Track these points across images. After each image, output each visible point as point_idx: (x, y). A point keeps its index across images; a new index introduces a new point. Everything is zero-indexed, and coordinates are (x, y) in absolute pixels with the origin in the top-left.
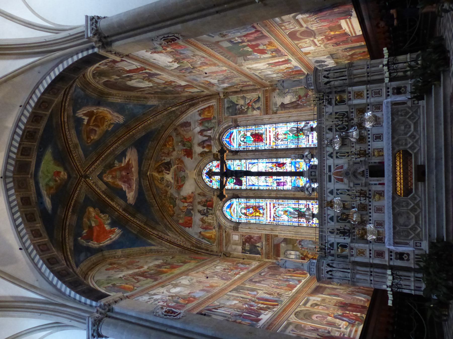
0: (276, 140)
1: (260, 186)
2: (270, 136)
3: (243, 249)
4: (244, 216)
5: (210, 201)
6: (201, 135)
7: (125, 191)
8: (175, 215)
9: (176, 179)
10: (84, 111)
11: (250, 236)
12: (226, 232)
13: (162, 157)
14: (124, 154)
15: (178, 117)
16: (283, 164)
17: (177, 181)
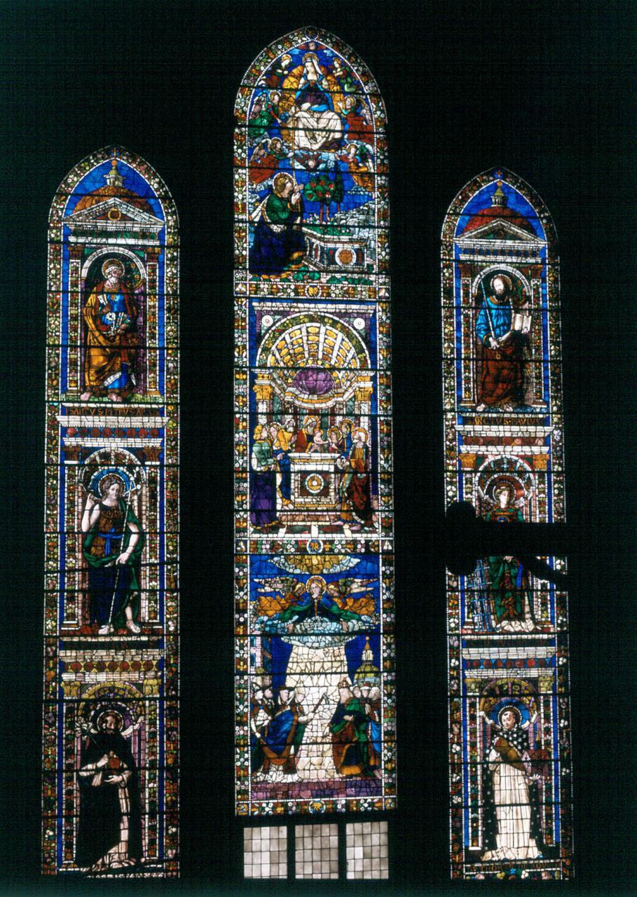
0: (487, 471)
1: (254, 377)
4: (84, 273)
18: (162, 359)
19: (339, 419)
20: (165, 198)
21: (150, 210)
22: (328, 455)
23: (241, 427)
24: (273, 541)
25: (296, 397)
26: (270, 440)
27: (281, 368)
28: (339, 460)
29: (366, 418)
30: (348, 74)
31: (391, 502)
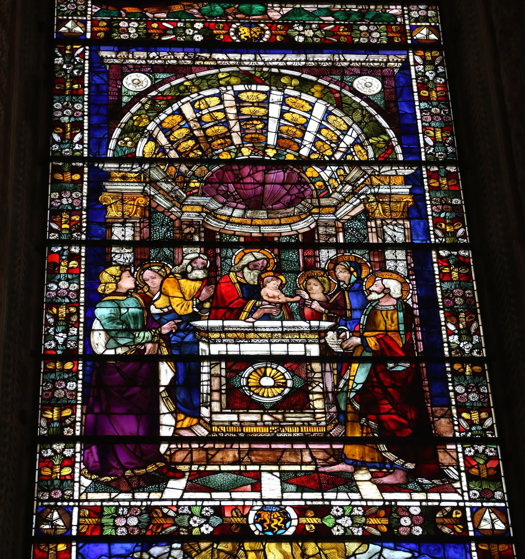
19: (325, 255)
22: (303, 324)
23: (63, 270)
24: (150, 510)
25: (212, 213)
26: (144, 296)
27: (172, 162)
28: (331, 334)
29: (401, 254)
31: (488, 423)
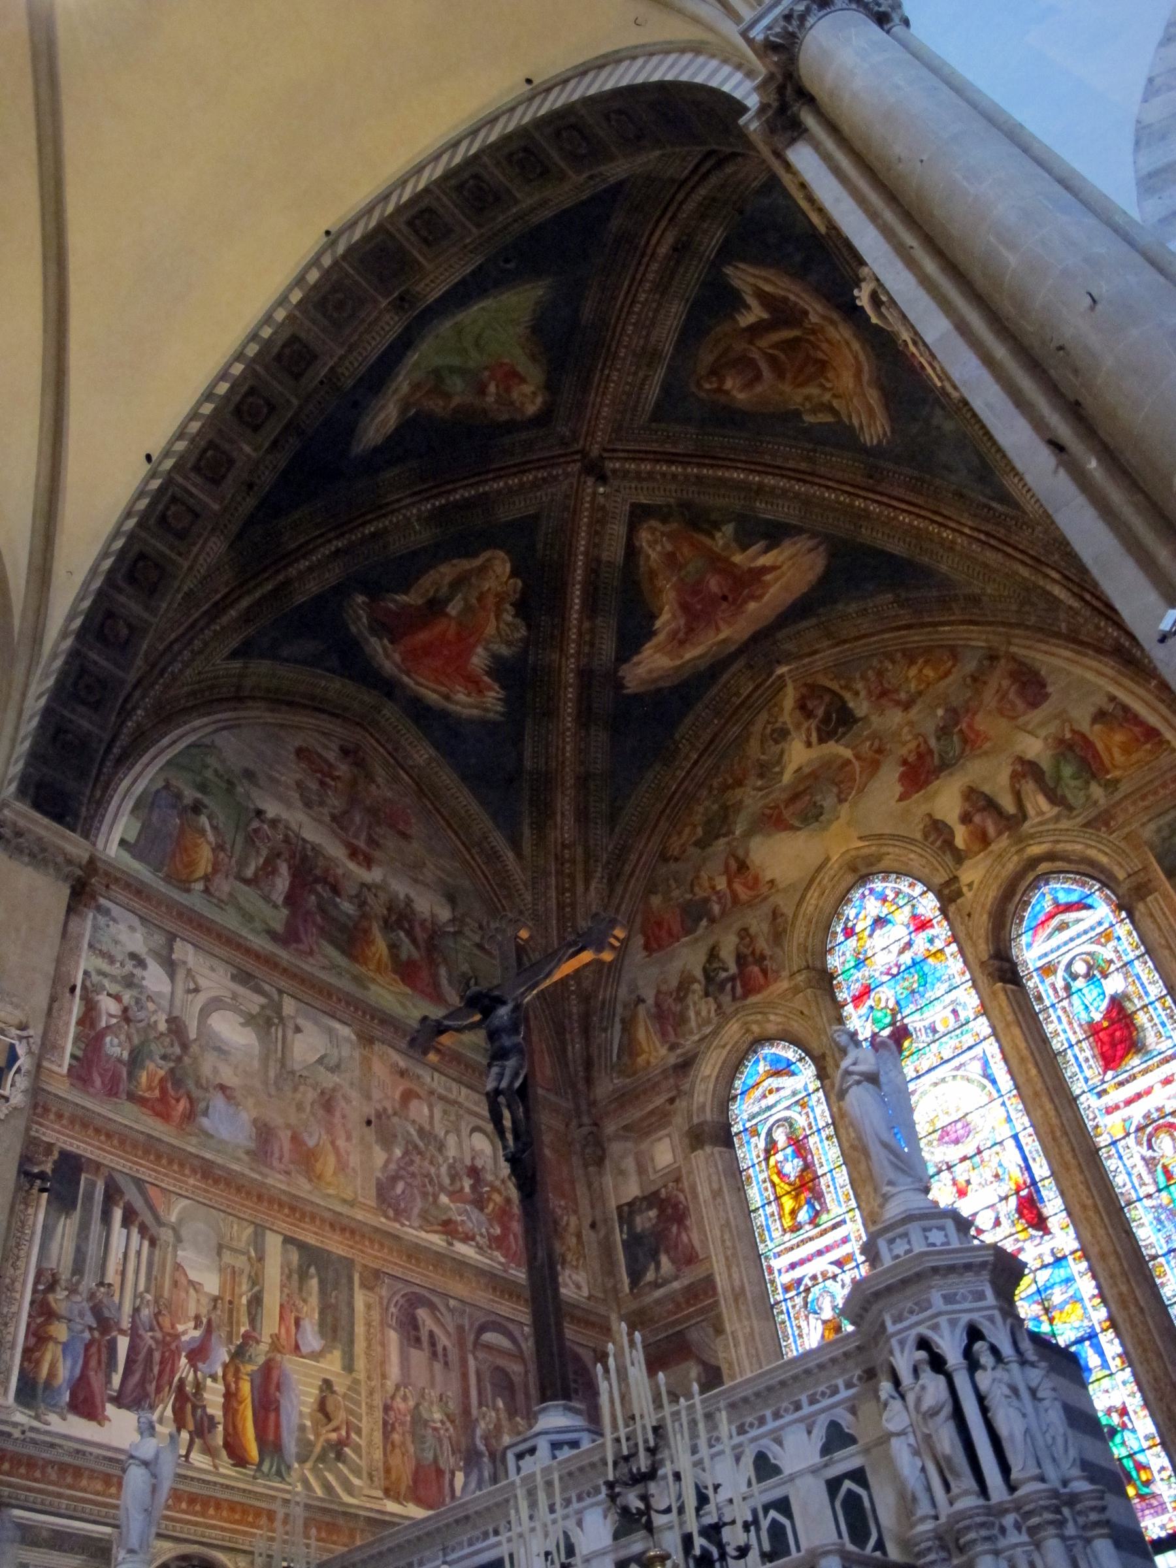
0: (1140, 1129)
2: (1148, 1091)
3: (630, 1204)
4: (762, 1144)
5: (765, 972)
6: (1015, 776)
7: (652, 634)
8: (673, 866)
9: (801, 787)
10: (766, 280)
11: (687, 1208)
12: (672, 1101)
13: (864, 677)
14: (775, 534)
15: (1047, 632)
16: (1039, 1223)
17: (795, 797)
18: (833, 1179)
20: (801, 1060)
21: (793, 1074)
30: (898, 893)
